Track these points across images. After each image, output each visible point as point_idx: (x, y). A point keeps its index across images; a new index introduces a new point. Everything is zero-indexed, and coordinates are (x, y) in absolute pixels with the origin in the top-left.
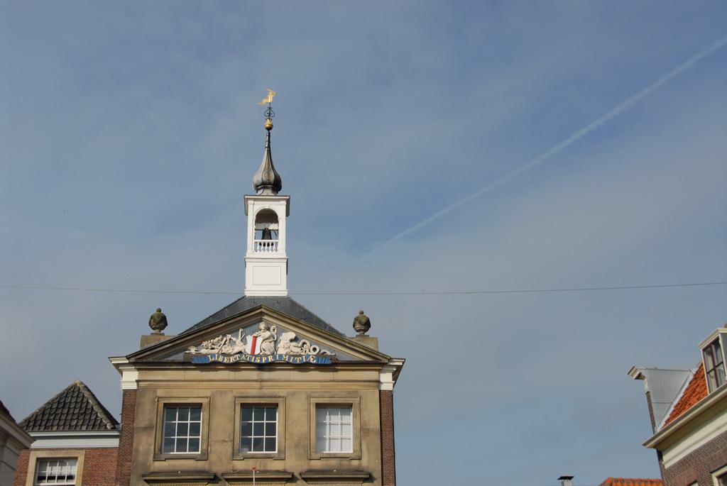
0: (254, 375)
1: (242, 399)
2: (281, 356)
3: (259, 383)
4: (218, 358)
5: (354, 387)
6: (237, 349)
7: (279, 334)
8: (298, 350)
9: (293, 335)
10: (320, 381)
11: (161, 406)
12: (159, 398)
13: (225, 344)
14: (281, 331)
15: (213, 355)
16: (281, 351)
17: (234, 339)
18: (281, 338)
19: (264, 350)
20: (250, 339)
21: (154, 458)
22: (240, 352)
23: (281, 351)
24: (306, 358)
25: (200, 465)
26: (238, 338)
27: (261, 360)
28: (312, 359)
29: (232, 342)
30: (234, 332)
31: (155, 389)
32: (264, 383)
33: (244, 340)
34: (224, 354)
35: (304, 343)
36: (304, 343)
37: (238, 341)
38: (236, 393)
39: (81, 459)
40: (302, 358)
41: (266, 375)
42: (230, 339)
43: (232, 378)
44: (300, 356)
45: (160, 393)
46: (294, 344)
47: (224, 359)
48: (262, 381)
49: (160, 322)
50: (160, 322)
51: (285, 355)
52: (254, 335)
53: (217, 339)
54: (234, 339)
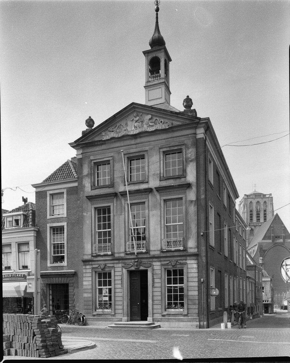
0: (133, 142)
1: (128, 155)
3: (135, 145)
5: (183, 139)
9: (150, 116)
10: (165, 139)
11: (92, 163)
12: (91, 160)
21: (91, 188)
31: (89, 157)
39: (65, 193)
41: (138, 140)
43: (122, 145)
45: (92, 158)
46: (151, 121)
49: (90, 122)
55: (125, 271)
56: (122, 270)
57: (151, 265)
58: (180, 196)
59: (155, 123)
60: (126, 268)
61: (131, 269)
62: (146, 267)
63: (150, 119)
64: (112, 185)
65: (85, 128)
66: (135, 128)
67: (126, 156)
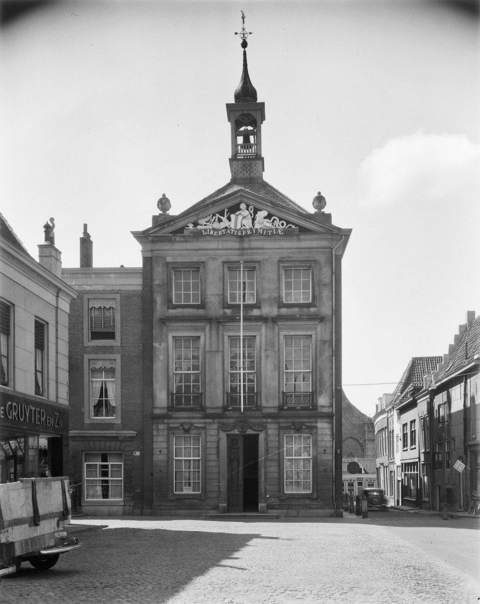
2: (257, 230)
4: (210, 232)
6: (222, 225)
7: (255, 213)
8: (269, 225)
9: (265, 213)
13: (214, 221)
14: (256, 211)
15: (206, 230)
16: (257, 226)
17: (222, 217)
18: (257, 215)
19: (244, 226)
20: (233, 216)
22: (226, 228)
23: (257, 226)
24: (276, 231)
25: (201, 312)
26: (224, 217)
27: (242, 233)
28: (280, 232)
29: (220, 221)
30: (222, 213)
32: (245, 251)
33: (229, 219)
34: (214, 229)
35: (274, 220)
36: (274, 220)
37: (224, 219)
38: (224, 259)
40: (273, 231)
42: (219, 218)
44: (272, 229)
46: (267, 220)
47: (214, 233)
48: (243, 249)
49: (164, 203)
50: (164, 203)
51: (260, 229)
52: (238, 213)
53: (208, 217)
54: (222, 217)
55: (223, 435)
56: (218, 432)
57: (264, 427)
58: (309, 333)
59: (273, 224)
60: (225, 431)
61: (230, 433)
62: (257, 431)
63: (265, 218)
64: (203, 306)
65: (158, 212)
66: (242, 227)
67: (226, 266)
